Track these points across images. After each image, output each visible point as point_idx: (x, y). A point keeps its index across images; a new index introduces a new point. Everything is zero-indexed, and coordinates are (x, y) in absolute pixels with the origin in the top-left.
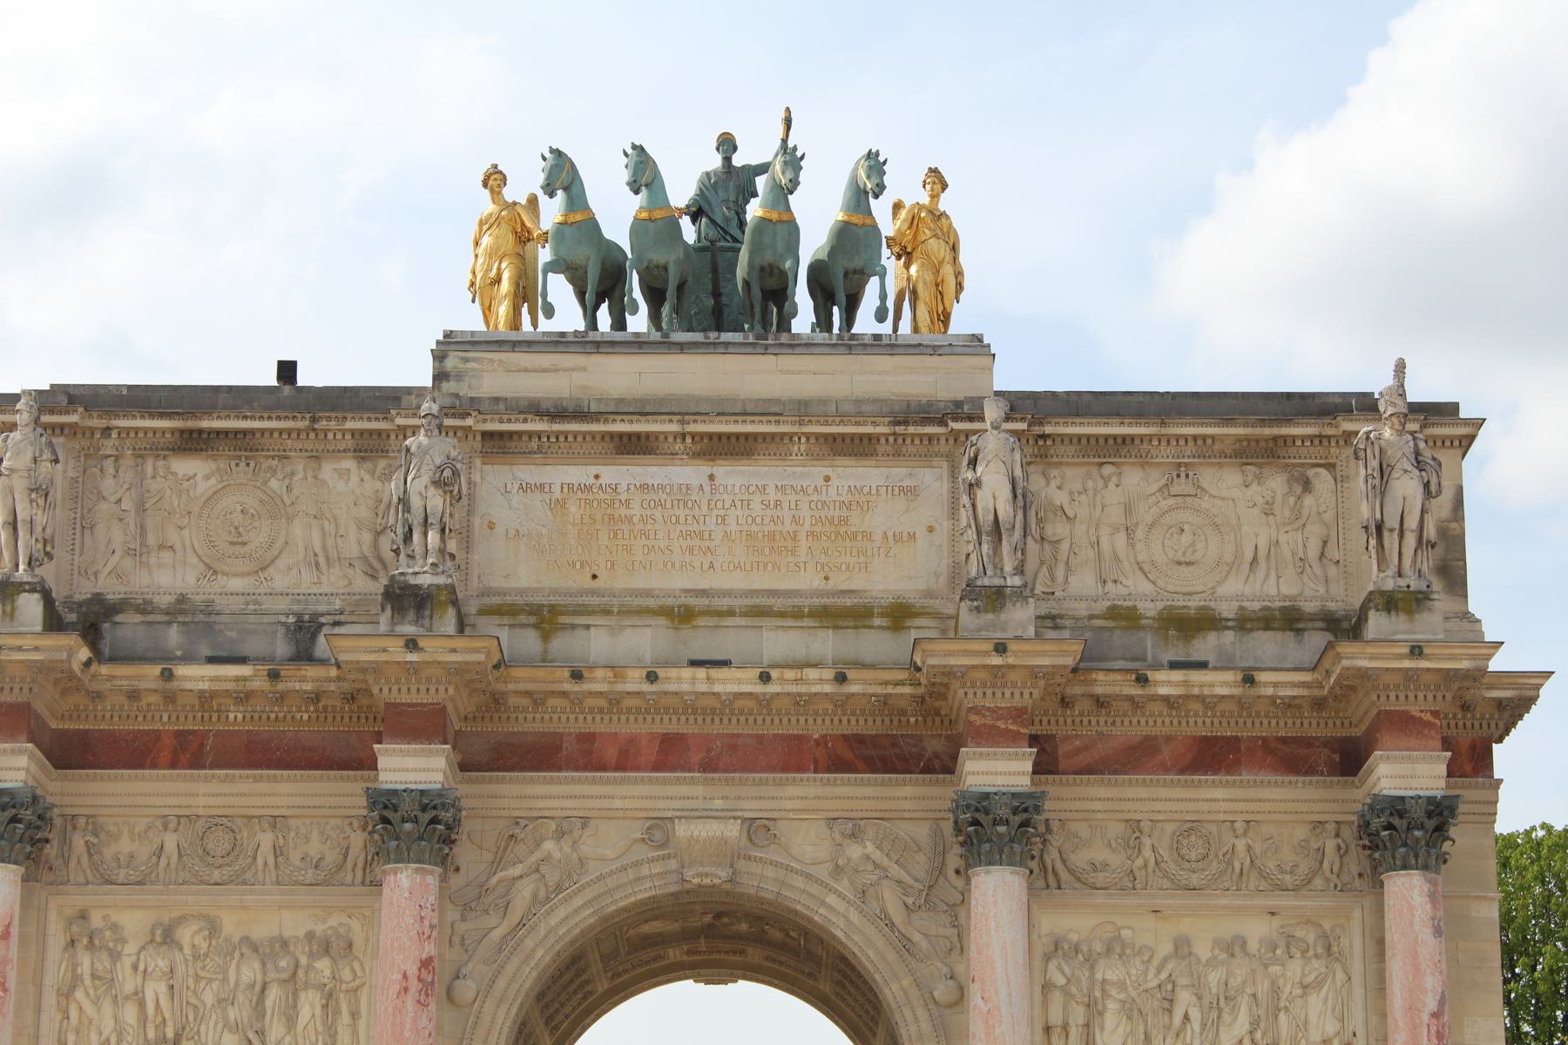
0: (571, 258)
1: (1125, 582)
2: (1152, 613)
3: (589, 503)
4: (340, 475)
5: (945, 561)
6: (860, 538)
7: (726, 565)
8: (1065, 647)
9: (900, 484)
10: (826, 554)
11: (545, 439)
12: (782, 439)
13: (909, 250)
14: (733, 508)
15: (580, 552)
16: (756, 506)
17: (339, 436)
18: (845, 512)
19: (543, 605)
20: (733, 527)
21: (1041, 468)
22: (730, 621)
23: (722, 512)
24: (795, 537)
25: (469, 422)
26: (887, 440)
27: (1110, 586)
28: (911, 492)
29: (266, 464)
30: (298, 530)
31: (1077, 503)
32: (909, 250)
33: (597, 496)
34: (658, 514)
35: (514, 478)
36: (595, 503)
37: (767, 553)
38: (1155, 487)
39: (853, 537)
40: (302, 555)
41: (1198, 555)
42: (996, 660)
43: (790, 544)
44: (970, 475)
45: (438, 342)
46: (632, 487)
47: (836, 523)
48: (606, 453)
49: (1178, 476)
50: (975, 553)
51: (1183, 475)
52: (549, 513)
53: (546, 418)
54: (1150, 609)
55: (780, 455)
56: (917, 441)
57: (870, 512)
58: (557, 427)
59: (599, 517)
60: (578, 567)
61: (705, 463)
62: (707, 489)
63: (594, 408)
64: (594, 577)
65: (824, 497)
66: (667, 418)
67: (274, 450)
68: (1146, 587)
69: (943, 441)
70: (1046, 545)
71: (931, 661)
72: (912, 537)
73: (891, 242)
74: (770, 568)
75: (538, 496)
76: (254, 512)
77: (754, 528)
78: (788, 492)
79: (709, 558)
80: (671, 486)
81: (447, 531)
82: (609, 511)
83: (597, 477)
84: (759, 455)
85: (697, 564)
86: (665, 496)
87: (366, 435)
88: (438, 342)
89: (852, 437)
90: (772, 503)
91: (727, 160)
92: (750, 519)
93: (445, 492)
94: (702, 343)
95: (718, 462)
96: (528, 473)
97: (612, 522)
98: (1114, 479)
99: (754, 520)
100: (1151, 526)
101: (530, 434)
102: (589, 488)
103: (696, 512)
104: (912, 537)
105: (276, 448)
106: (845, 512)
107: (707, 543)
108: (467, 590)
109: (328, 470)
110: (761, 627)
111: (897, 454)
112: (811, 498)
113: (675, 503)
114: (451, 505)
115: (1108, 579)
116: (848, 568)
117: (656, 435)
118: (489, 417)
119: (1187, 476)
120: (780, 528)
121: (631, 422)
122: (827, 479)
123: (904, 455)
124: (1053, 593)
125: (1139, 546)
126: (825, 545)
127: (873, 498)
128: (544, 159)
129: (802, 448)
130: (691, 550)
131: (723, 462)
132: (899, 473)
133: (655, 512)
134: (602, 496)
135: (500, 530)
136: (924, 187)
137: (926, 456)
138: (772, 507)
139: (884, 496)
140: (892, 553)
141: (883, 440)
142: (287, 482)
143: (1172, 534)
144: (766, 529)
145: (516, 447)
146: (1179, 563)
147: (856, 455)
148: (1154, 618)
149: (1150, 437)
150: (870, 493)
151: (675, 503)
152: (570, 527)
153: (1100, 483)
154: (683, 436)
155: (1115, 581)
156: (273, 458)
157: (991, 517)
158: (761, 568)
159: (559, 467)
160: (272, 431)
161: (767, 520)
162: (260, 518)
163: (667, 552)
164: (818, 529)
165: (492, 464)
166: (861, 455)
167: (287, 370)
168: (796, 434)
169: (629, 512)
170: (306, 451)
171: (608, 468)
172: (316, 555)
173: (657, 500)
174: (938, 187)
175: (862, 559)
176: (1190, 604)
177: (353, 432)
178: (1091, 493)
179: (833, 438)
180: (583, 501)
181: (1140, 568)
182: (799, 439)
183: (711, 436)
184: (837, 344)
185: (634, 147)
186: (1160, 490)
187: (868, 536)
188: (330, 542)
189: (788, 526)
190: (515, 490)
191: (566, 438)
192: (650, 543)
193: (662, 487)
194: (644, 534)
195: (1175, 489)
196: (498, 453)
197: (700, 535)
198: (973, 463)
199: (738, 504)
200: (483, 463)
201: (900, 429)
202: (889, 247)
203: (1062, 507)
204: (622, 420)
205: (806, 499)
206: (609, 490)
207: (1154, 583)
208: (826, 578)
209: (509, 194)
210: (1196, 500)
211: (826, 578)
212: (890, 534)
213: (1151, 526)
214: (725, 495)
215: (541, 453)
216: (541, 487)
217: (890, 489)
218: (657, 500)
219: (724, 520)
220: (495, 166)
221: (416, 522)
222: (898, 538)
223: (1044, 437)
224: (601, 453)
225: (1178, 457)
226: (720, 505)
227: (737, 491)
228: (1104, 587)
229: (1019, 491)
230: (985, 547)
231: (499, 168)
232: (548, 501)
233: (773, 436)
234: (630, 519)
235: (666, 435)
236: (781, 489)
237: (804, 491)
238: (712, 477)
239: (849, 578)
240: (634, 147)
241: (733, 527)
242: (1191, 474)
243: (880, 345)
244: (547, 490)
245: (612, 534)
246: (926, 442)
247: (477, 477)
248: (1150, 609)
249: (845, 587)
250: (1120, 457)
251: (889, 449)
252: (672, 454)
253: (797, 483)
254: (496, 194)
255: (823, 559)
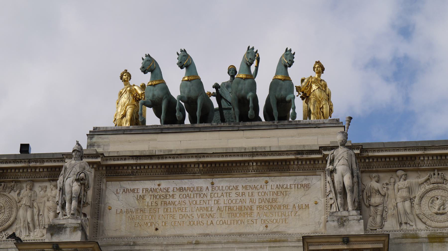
0: (154, 99)
1: (411, 223)
2: (425, 236)
3: (155, 197)
4: (42, 189)
5: (323, 217)
6: (282, 208)
7: (218, 222)
8: (378, 239)
9: (301, 183)
10: (266, 216)
11: (135, 168)
12: (244, 164)
13: (308, 95)
14: (222, 197)
15: (150, 218)
16: (233, 195)
17: (41, 170)
18: (275, 196)
19: (131, 242)
20: (222, 205)
21: (368, 174)
22: (220, 246)
23: (217, 199)
24: (251, 209)
25: (99, 160)
26: (294, 162)
27: (404, 227)
28: (307, 187)
29: (9, 185)
30: (21, 212)
31: (386, 188)
32: (308, 95)
33: (159, 193)
34: (187, 200)
35: (121, 187)
36: (158, 197)
37: (238, 216)
38: (422, 179)
39: (279, 207)
40: (22, 224)
41: (446, 211)
42: (345, 247)
43: (249, 211)
44: (331, 167)
45: (90, 132)
46: (175, 189)
47: (271, 201)
48: (163, 174)
49: (434, 174)
50: (334, 204)
51: (436, 173)
52: (136, 202)
53: (135, 158)
54: (423, 234)
55: (244, 172)
56: (308, 162)
57: (287, 196)
58: (139, 162)
59: (159, 203)
60: (149, 225)
61: (209, 177)
62: (210, 188)
63: (157, 154)
64: (157, 229)
65: (265, 190)
66: (191, 155)
67: (12, 178)
68: (422, 226)
69: (320, 162)
70: (372, 208)
71: (311, 248)
72: (307, 206)
73: (298, 89)
74: (239, 222)
75: (132, 194)
76: (2, 206)
77: (232, 205)
78: (248, 188)
79: (211, 219)
80: (194, 188)
81: (82, 203)
82: (164, 200)
83: (159, 185)
84: (234, 172)
85: (205, 222)
86: (190, 192)
87: (53, 169)
88: (90, 132)
89: (278, 161)
90: (240, 193)
91: (233, 77)
92: (230, 201)
93: (81, 184)
94: (209, 127)
95: (215, 176)
96: (128, 185)
97: (165, 205)
98: (403, 177)
99: (232, 201)
100: (421, 198)
101: (128, 165)
102: (155, 190)
103: (205, 198)
104: (307, 206)
105: (14, 177)
106: (275, 196)
107: (210, 212)
108: (96, 236)
109: (37, 187)
110: (235, 247)
111: (299, 169)
112: (259, 191)
113: (195, 195)
114: (85, 190)
115: (403, 222)
116: (277, 222)
117: (186, 163)
118: (109, 158)
119: (438, 174)
120: (244, 204)
121: (174, 158)
122: (267, 182)
123: (303, 170)
124: (376, 230)
125: (416, 207)
126: (266, 212)
127: (288, 190)
128: (143, 59)
129: (254, 167)
130: (202, 216)
131: (218, 176)
132: (301, 179)
133: (186, 199)
134: (161, 193)
135: (113, 210)
136: (314, 70)
137: (313, 170)
138: (240, 195)
139: (293, 189)
140: (298, 214)
141: (292, 163)
142: (18, 192)
143: (433, 201)
144: (238, 205)
145: (122, 173)
146: (437, 214)
147: (279, 171)
148: (426, 238)
149: (419, 156)
150: (287, 188)
151: (195, 195)
152: (146, 207)
153: (397, 180)
154: (198, 163)
155: (406, 223)
156: (12, 181)
157: (342, 185)
158: (235, 223)
159: (142, 181)
160: (11, 168)
161: (238, 201)
162: (4, 208)
163: (191, 217)
164: (263, 204)
165: (111, 181)
166: (282, 171)
167: (25, 148)
168: (250, 161)
169: (173, 200)
170: (27, 178)
171: (164, 181)
172: (28, 223)
173: (187, 194)
174: (320, 69)
175: (283, 217)
176: (444, 231)
177: (47, 167)
178: (392, 184)
179: (269, 161)
180: (152, 196)
181: (418, 217)
182: (253, 164)
183: (211, 163)
184: (271, 125)
185: (181, 51)
186: (426, 181)
187: (286, 206)
188: (36, 217)
189: (248, 204)
190: (121, 193)
191: (144, 167)
192: (183, 213)
193: (189, 189)
194: (180, 209)
195: (432, 180)
196: (113, 176)
197: (207, 209)
198: (332, 162)
199: (225, 195)
200: (107, 181)
201: (299, 156)
202: (297, 91)
203: (378, 190)
204: (170, 157)
205: (257, 191)
206: (164, 191)
207: (425, 223)
208: (267, 227)
209: (131, 82)
210: (443, 185)
211: (267, 227)
212: (296, 205)
213: (421, 198)
214: (219, 191)
215: (133, 175)
216: (133, 191)
217: (296, 185)
218: (187, 194)
219: (218, 202)
220: (126, 70)
221: (68, 198)
222: (300, 207)
223: (369, 157)
224: (161, 174)
225: (434, 166)
226: (216, 195)
227: (224, 189)
228: (400, 226)
229: (355, 174)
230: (339, 200)
231: (128, 71)
232: (136, 197)
233: (240, 162)
234: (174, 203)
235: (190, 163)
236: (245, 187)
237: (255, 188)
238: (212, 184)
239: (278, 226)
240: (181, 51)
241: (222, 205)
242: (440, 173)
243: (291, 124)
244: (136, 191)
245: (165, 210)
246: (312, 162)
247: (103, 187)
248: (423, 234)
249: (275, 230)
250: (406, 167)
251: (295, 166)
252: (194, 173)
253: (252, 184)
254: (126, 82)
255: (265, 218)
